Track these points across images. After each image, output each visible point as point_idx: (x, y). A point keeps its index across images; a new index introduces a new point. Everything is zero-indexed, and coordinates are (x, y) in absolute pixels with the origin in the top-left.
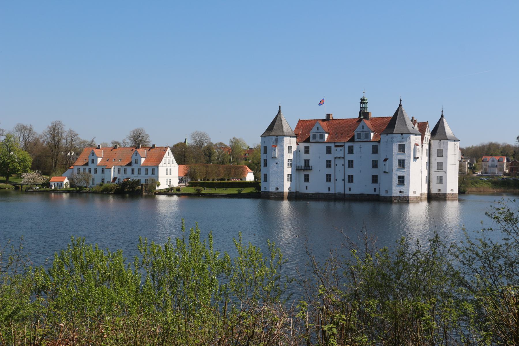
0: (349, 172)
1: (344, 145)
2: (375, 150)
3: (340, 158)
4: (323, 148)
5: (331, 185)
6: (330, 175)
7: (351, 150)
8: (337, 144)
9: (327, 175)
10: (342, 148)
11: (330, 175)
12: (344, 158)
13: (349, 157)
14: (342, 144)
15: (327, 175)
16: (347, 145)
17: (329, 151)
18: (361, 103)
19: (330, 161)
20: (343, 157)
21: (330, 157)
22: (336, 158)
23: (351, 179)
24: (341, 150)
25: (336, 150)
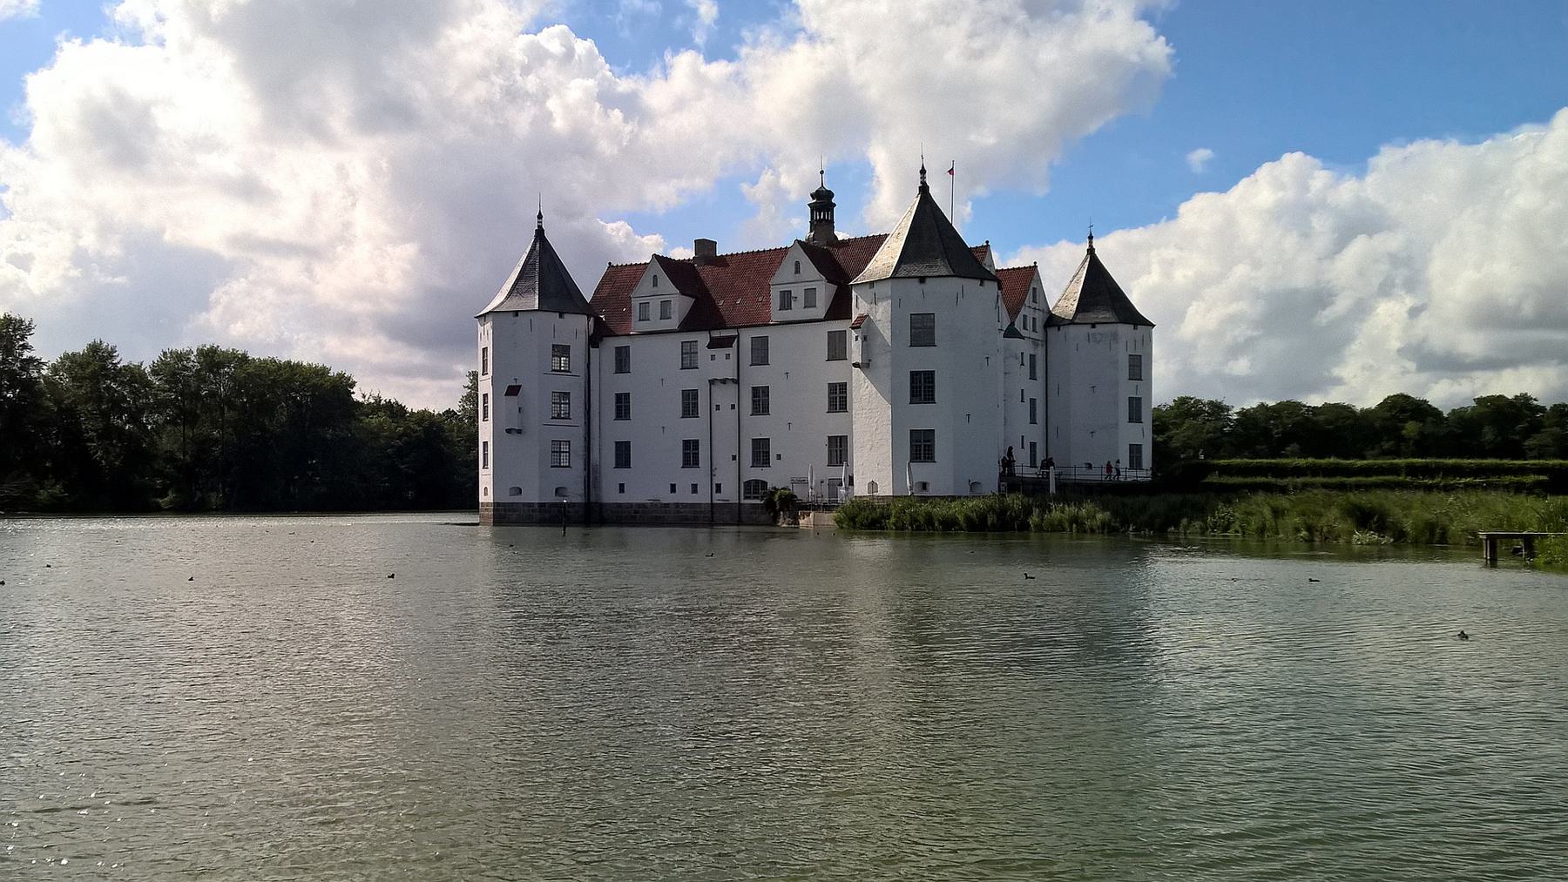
0: (759, 427)
1: (738, 336)
2: (837, 349)
3: (724, 381)
4: (672, 347)
5: (699, 475)
6: (696, 442)
7: (761, 354)
8: (716, 334)
9: (686, 443)
10: (732, 351)
11: (696, 442)
12: (737, 382)
13: (756, 376)
14: (733, 333)
15: (686, 443)
16: (747, 336)
17: (689, 360)
18: (814, 208)
19: (695, 393)
20: (732, 375)
21: (691, 380)
22: (712, 382)
23: (761, 454)
24: (728, 356)
25: (713, 357)
